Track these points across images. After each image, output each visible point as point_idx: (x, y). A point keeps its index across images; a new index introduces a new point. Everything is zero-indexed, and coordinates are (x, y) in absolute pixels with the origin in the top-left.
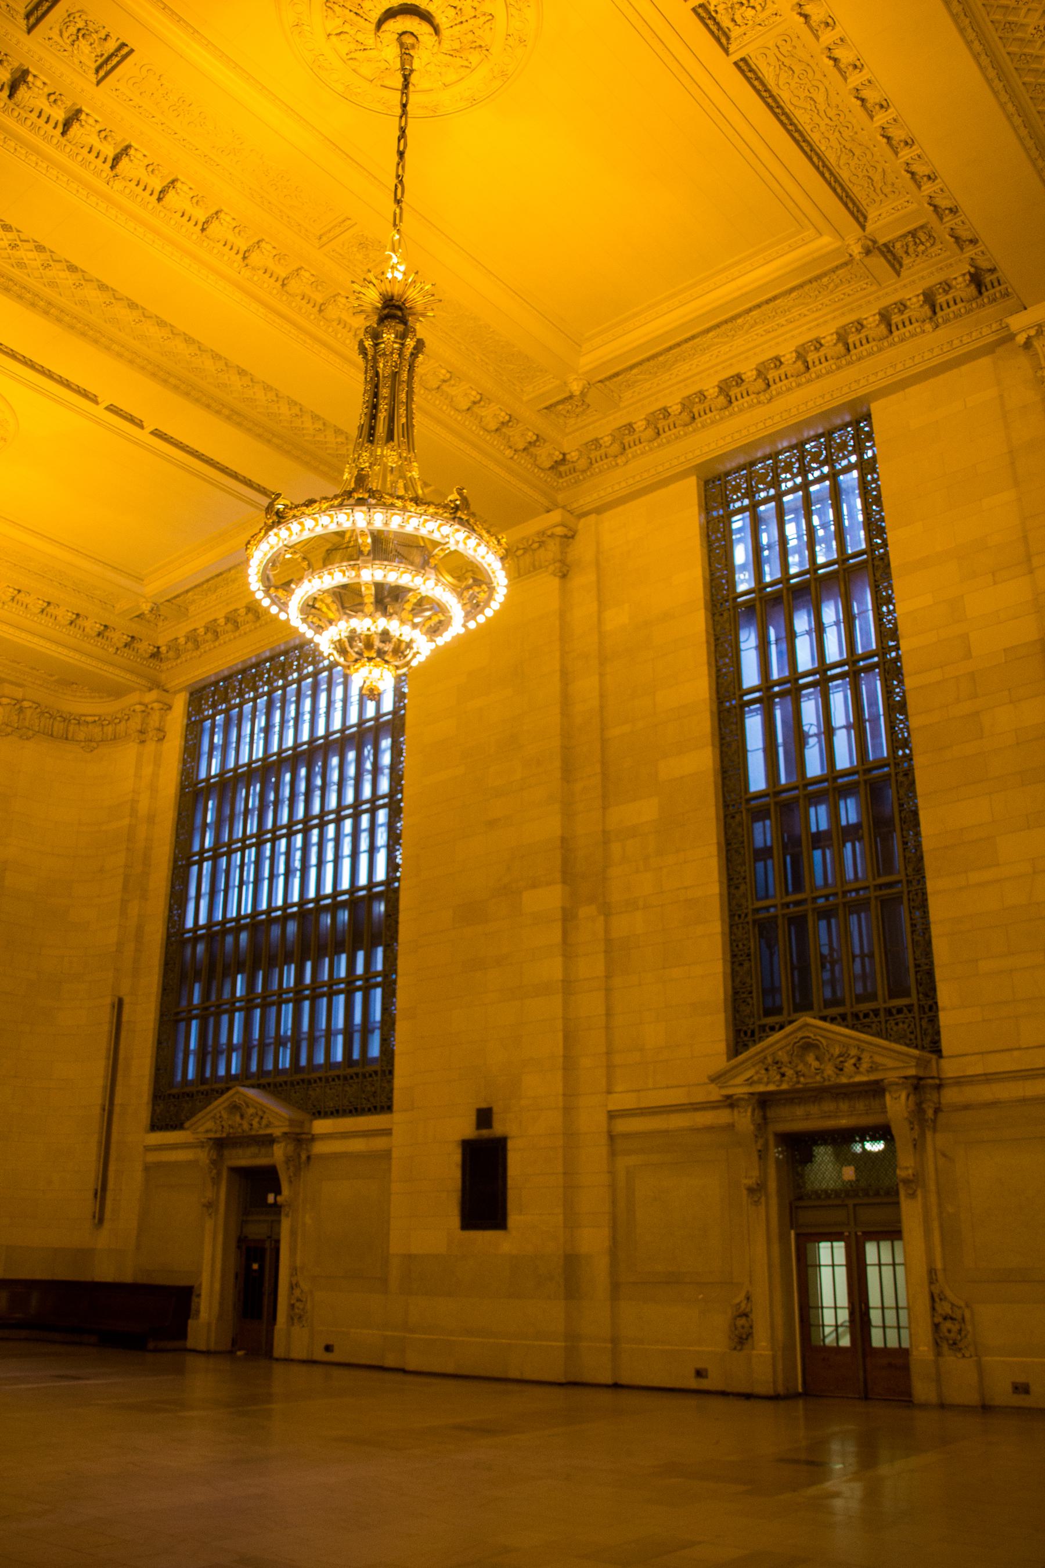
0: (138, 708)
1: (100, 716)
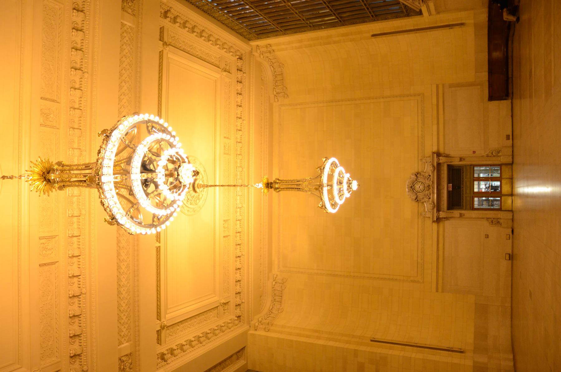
0: (262, 57)
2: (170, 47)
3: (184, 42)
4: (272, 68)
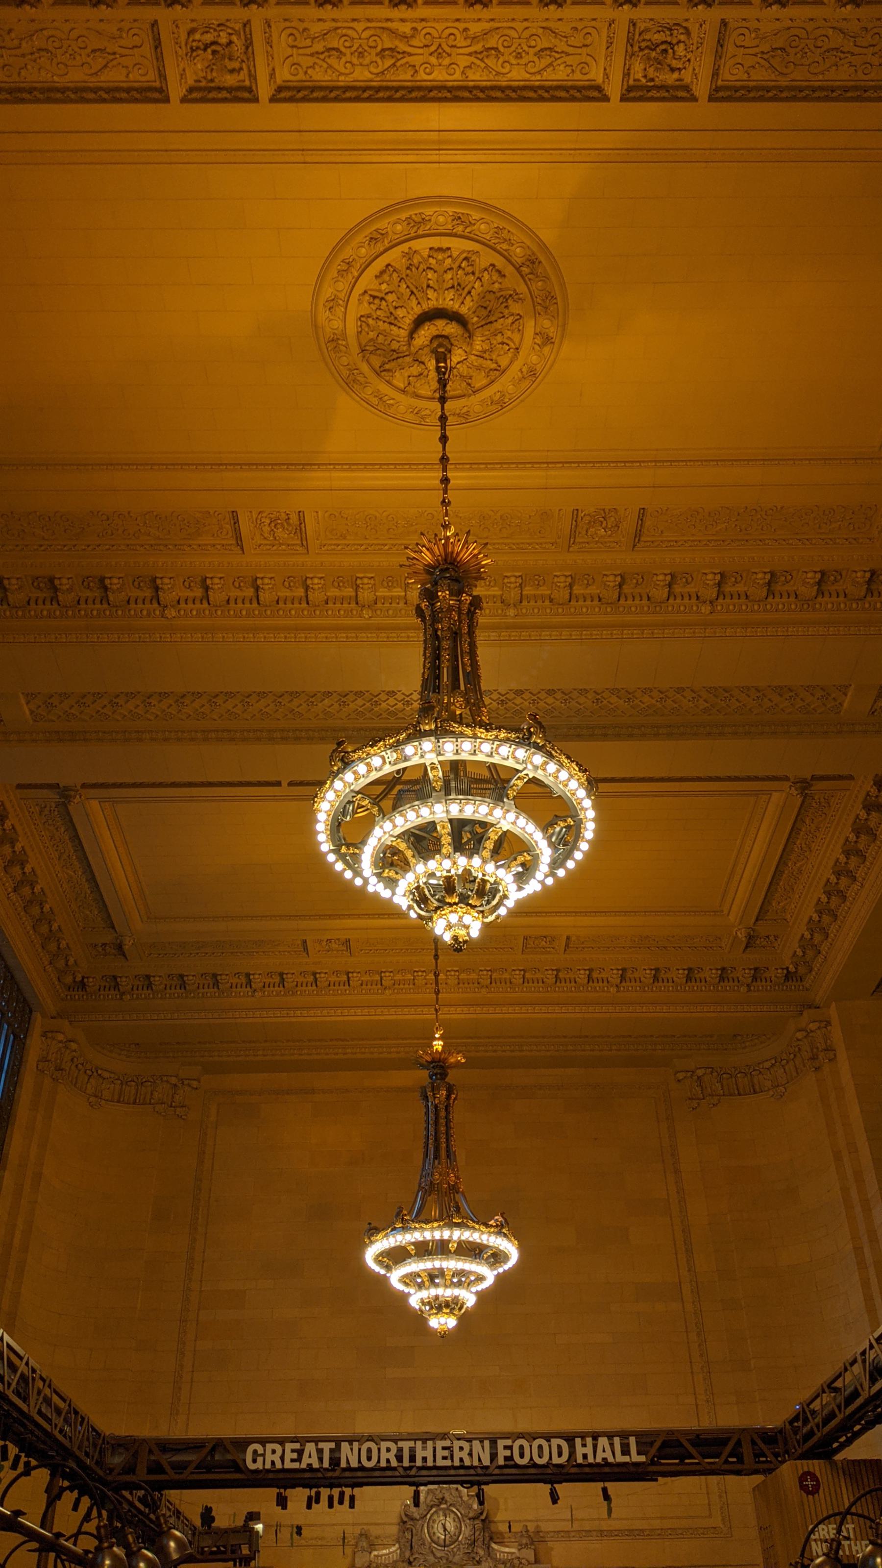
0: (799, 1035)
1: (775, 1058)
2: (799, 799)
3: (818, 828)
4: (767, 1064)
